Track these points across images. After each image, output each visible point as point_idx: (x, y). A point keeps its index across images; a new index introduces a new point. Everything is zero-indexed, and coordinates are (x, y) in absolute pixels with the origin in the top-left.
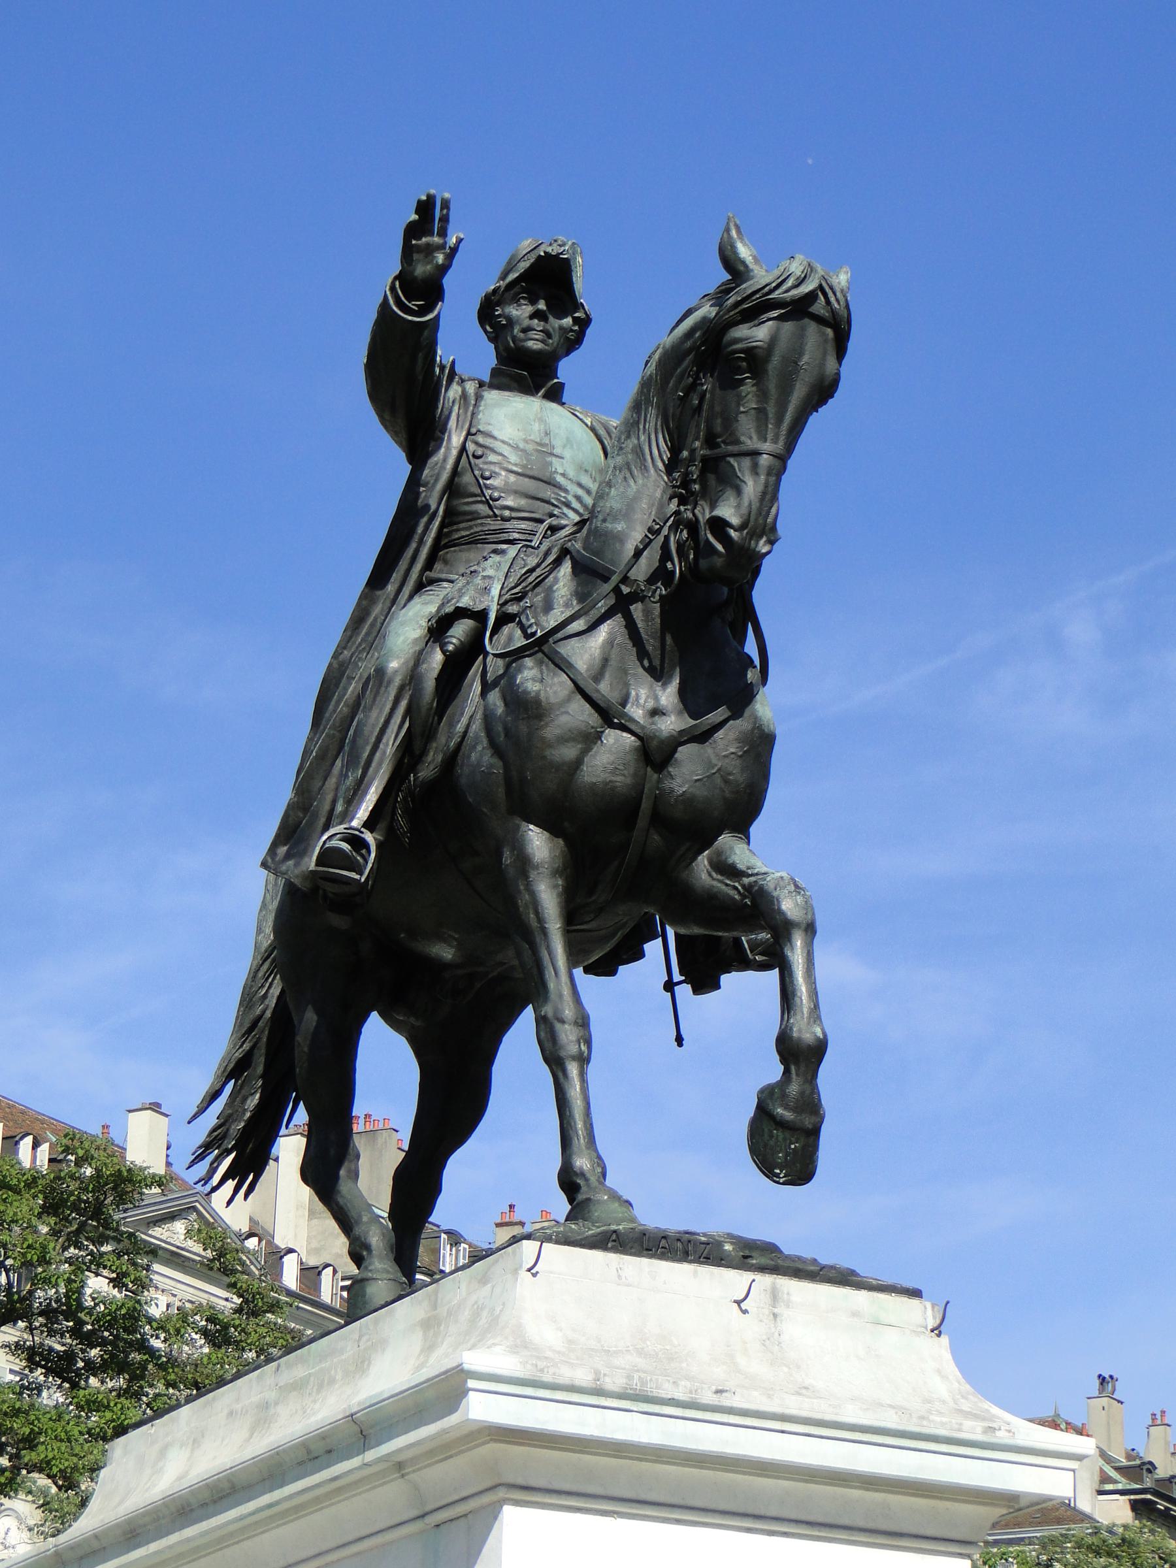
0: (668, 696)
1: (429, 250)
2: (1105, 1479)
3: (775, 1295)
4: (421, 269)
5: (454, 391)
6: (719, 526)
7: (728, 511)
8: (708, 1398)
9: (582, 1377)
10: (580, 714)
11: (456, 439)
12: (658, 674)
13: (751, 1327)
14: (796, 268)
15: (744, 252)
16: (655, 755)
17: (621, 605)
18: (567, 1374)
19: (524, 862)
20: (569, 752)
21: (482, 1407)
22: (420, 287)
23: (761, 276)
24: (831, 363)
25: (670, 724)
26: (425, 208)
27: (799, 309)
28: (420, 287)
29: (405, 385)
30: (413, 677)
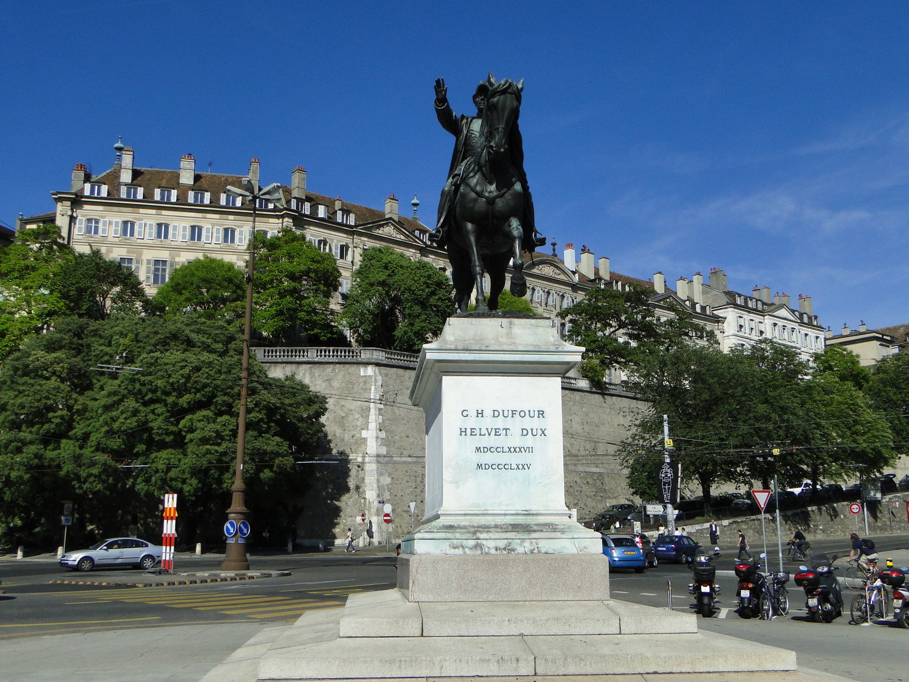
0: (493, 187)
1: (441, 91)
3: (511, 323)
4: (440, 96)
5: (465, 121)
6: (491, 147)
7: (492, 144)
8: (484, 348)
9: (452, 347)
10: (473, 195)
11: (465, 132)
12: (491, 184)
13: (504, 331)
14: (503, 82)
15: (492, 80)
16: (491, 202)
17: (480, 169)
18: (448, 347)
19: (467, 232)
20: (471, 205)
22: (441, 99)
23: (496, 85)
24: (515, 103)
25: (495, 194)
26: (438, 82)
27: (504, 92)
28: (441, 99)
29: (450, 122)
30: (450, 191)
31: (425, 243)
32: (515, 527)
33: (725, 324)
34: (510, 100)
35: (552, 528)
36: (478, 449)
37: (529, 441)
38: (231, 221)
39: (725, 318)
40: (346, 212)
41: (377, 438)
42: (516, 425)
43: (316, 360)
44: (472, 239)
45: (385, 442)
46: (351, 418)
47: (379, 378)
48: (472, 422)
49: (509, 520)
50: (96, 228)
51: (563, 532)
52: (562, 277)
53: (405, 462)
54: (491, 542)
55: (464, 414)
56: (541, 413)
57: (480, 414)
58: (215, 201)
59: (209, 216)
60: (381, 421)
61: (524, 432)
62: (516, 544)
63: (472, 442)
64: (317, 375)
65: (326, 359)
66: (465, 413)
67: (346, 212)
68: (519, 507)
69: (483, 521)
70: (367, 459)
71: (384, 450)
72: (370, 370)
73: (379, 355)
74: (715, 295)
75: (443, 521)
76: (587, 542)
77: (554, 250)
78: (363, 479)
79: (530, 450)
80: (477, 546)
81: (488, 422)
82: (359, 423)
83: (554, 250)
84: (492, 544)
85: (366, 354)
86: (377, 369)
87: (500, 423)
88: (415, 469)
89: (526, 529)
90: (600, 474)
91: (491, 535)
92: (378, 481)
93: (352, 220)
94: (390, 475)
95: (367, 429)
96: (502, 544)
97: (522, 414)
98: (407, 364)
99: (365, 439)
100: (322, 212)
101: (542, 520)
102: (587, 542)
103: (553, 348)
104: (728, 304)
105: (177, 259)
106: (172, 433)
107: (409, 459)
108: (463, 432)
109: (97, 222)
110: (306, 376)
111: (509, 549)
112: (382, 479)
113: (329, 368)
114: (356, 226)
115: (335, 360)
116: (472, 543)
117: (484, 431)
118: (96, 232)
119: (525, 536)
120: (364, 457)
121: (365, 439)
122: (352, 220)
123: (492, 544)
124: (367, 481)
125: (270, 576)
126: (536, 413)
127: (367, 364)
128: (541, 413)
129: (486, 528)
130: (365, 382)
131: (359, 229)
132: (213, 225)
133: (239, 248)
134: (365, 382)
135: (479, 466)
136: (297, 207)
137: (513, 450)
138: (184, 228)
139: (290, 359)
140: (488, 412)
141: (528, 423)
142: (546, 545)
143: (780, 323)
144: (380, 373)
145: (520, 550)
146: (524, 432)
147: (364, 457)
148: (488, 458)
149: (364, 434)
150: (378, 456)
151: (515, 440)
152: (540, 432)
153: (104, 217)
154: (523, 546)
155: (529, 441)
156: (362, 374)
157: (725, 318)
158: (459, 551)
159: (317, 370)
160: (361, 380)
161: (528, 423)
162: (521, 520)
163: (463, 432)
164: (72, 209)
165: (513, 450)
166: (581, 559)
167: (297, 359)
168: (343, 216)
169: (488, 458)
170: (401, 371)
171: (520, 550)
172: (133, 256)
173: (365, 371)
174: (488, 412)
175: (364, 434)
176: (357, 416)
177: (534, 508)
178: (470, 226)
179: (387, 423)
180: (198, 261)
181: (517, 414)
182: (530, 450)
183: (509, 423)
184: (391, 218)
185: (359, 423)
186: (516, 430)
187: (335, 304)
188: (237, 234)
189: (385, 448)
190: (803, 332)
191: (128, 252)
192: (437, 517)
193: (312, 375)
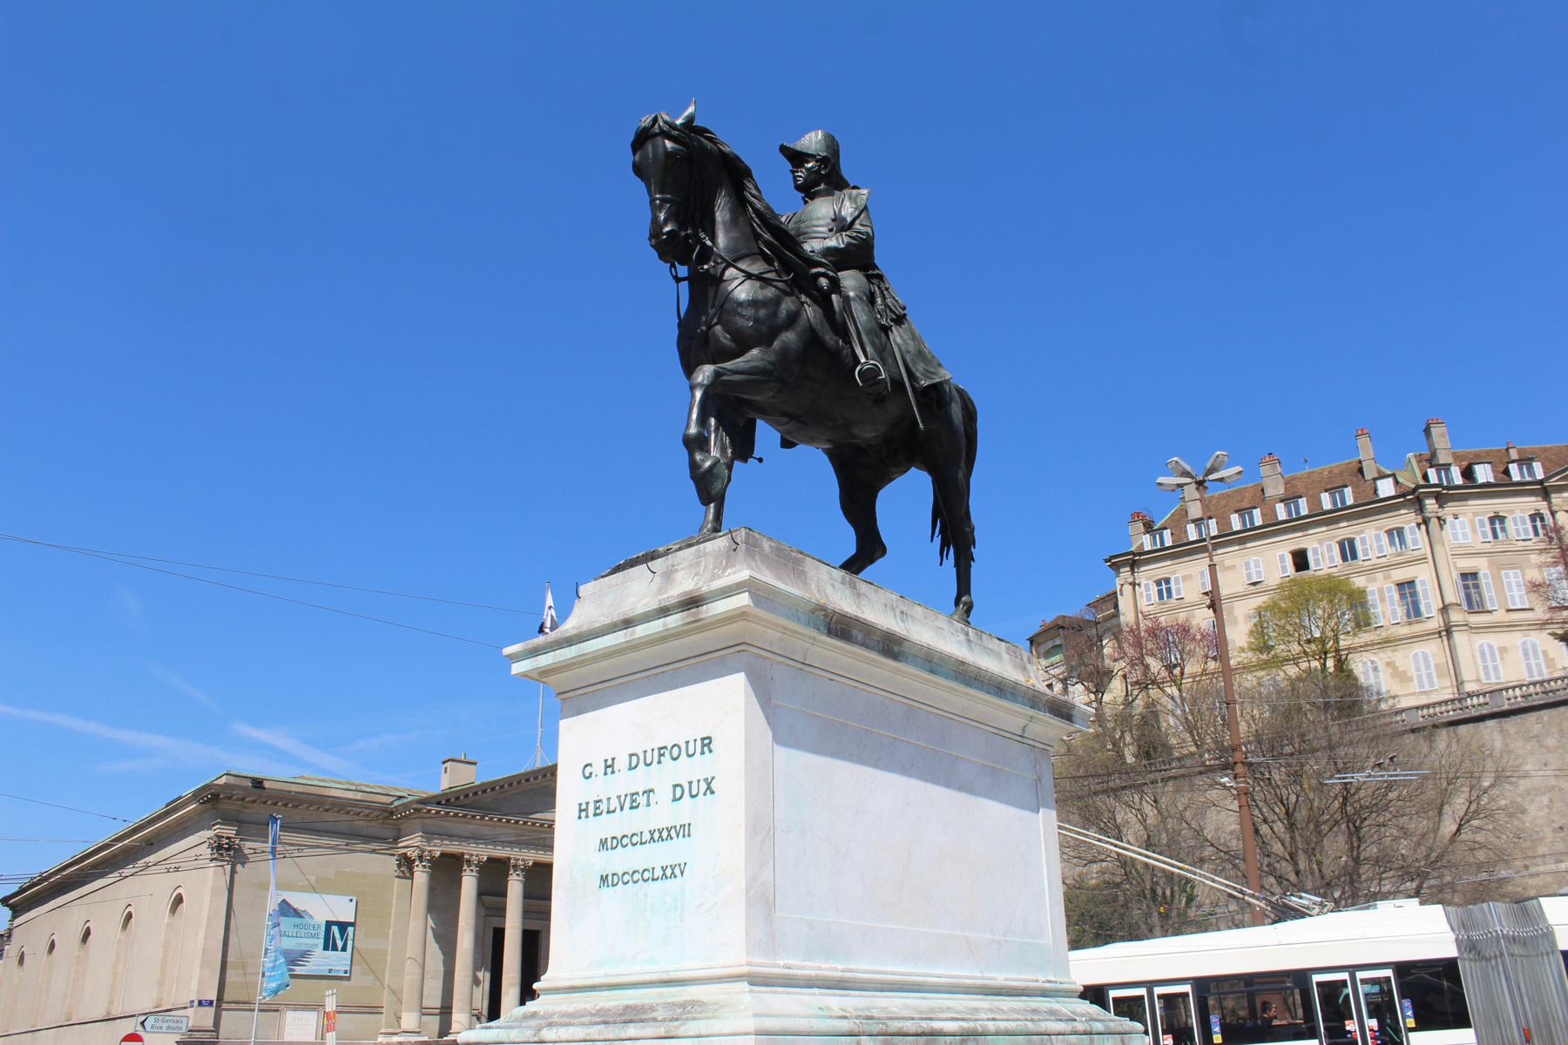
36: (603, 843)
38: (1344, 530)
40: (1525, 461)
42: (662, 777)
50: (1169, 590)
57: (609, 766)
64: (1512, 731)
66: (588, 770)
67: (1525, 461)
79: (684, 830)
81: (625, 782)
87: (638, 780)
93: (1539, 472)
100: (1483, 474)
109: (1167, 581)
114: (1547, 479)
117: (614, 804)
118: (1170, 596)
122: (1539, 472)
126: (699, 743)
128: (707, 742)
131: (1553, 482)
136: (1440, 478)
137: (660, 835)
140: (622, 763)
141: (689, 770)
148: (620, 860)
151: (662, 813)
152: (703, 786)
153: (1174, 572)
155: (684, 811)
161: (689, 770)
164: (1133, 572)
165: (660, 835)
168: (1521, 469)
169: (620, 860)
174: (622, 763)
181: (667, 753)
182: (684, 830)
186: (664, 794)
188: (1358, 544)
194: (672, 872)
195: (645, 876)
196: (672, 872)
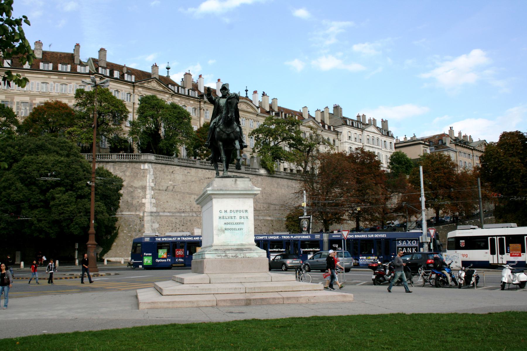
2: (451, 141)
21: (209, 192)
31: (174, 92)
32: (238, 249)
33: (341, 136)
34: (235, 101)
35: (250, 249)
36: (225, 224)
37: (242, 220)
39: (341, 132)
41: (151, 203)
42: (238, 215)
43: (117, 160)
44: (222, 147)
45: (156, 205)
46: (136, 192)
47: (152, 170)
48: (223, 214)
49: (236, 247)
51: (254, 250)
52: (250, 110)
53: (166, 216)
54: (230, 254)
55: (220, 211)
56: (246, 211)
57: (226, 211)
58: (55, 69)
59: (52, 77)
60: (153, 193)
61: (241, 218)
62: (238, 255)
63: (223, 221)
64: (117, 168)
65: (122, 160)
68: (239, 242)
69: (229, 247)
70: (145, 214)
71: (154, 210)
72: (146, 166)
73: (152, 157)
74: (336, 120)
75: (214, 248)
76: (262, 254)
77: (247, 94)
78: (144, 225)
79: (243, 223)
80: (225, 256)
81: (228, 214)
82: (141, 195)
83: (247, 94)
84: (230, 255)
85: (144, 157)
86: (150, 165)
87: (232, 214)
88: (172, 219)
89: (242, 250)
90: (272, 221)
91: (230, 252)
92: (152, 226)
94: (158, 223)
95: (145, 198)
96: (234, 255)
97: (240, 211)
98: (166, 162)
99: (144, 204)
101: (247, 247)
102: (262, 254)
103: (250, 189)
104: (343, 125)
105: (34, 102)
106: (42, 201)
107: (168, 214)
108: (220, 218)
110: (110, 168)
111: (236, 256)
112: (154, 225)
113: (124, 165)
115: (127, 160)
116: (224, 255)
119: (241, 252)
120: (144, 214)
121: (144, 204)
123: (230, 255)
124: (145, 226)
125: (110, 274)
127: (145, 162)
128: (246, 211)
129: (229, 250)
130: (144, 173)
132: (54, 82)
133: (70, 95)
134: (144, 173)
135: (226, 229)
138: (38, 84)
139: (102, 160)
141: (242, 214)
142: (248, 255)
143: (371, 135)
144: (152, 167)
145: (240, 257)
146: (241, 218)
147: (144, 214)
148: (228, 226)
149: (144, 201)
150: (152, 212)
151: (238, 220)
154: (240, 255)
155: (242, 220)
156: (142, 168)
157: (341, 132)
158: (220, 257)
159: (117, 167)
160: (141, 171)
161: (242, 214)
162: (240, 247)
163: (220, 218)
166: (259, 259)
167: (106, 160)
169: (228, 226)
170: (163, 166)
171: (240, 257)
172: (9, 100)
173: (144, 166)
175: (144, 201)
176: (139, 191)
177: (244, 243)
178: (221, 143)
179: (156, 194)
180: (47, 104)
182: (243, 223)
183: (235, 214)
184: (155, 78)
185: (141, 195)
186: (238, 217)
187: (126, 127)
189: (155, 208)
190: (383, 140)
191: (6, 98)
192: (212, 246)
193: (115, 169)
194: (240, 229)
195: (234, 229)
196: (240, 229)
